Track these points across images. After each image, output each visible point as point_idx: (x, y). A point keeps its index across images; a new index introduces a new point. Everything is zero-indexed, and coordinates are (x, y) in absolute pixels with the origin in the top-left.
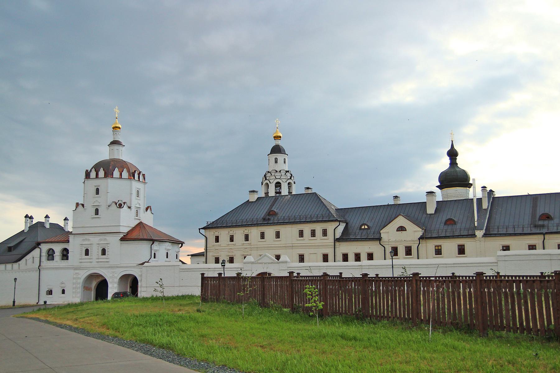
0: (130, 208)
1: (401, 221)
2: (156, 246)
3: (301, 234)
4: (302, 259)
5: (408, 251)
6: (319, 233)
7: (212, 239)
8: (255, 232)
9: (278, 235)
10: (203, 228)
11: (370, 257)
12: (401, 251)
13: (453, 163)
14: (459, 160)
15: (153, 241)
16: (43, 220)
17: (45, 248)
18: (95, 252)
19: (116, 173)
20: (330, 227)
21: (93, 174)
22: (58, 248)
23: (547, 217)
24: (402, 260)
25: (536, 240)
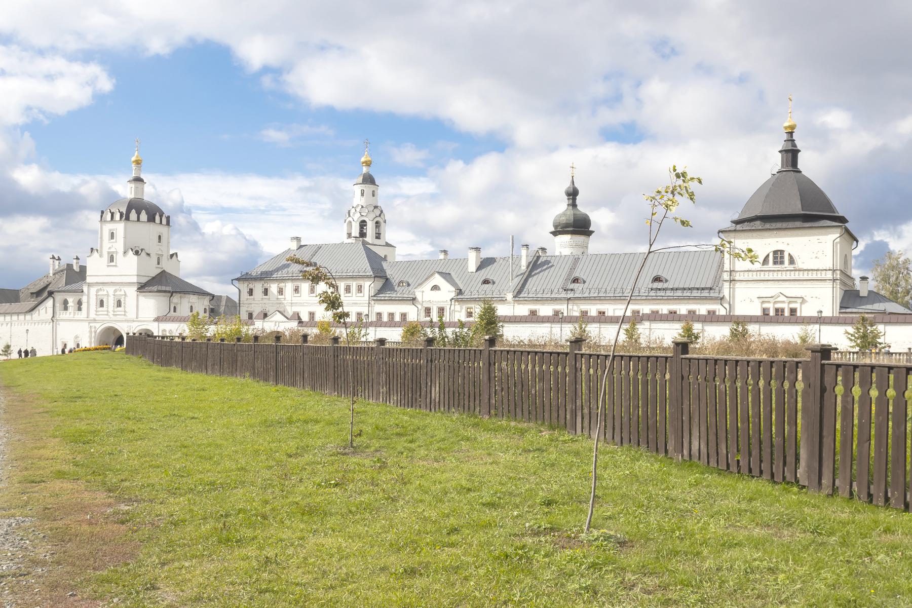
0: (148, 255)
2: (176, 299)
10: (237, 279)
13: (574, 205)
14: (579, 199)
17: (59, 297)
18: (110, 303)
19: (133, 215)
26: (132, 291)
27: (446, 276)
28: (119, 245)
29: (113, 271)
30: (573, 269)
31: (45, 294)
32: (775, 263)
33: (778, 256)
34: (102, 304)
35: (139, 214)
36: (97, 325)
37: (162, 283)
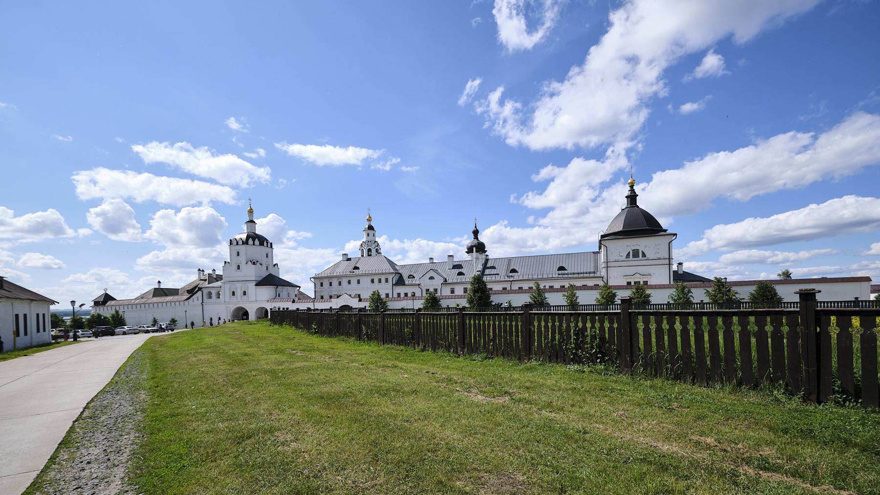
3: (373, 281)
6: (383, 280)
7: (319, 284)
9: (359, 282)
13: (476, 237)
16: (211, 272)
18: (239, 293)
28: (242, 259)
29: (239, 273)
32: (634, 256)
33: (636, 254)
36: (231, 306)
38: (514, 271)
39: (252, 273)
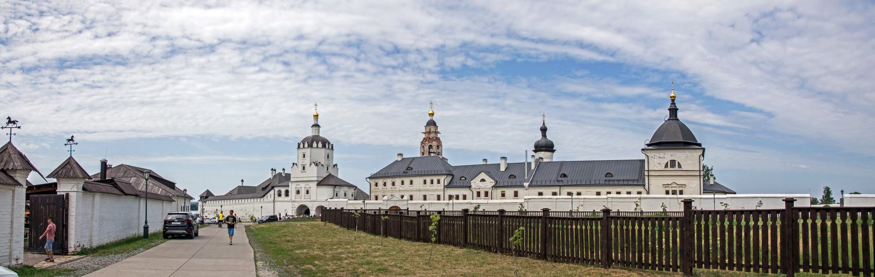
1: (483, 175)
2: (337, 189)
3: (425, 182)
4: (425, 198)
5: (486, 194)
6: (435, 181)
8: (398, 181)
9: (411, 183)
11: (465, 197)
12: (482, 194)
15: (335, 186)
17: (277, 189)
18: (303, 192)
19: (315, 145)
20: (442, 178)
21: (302, 146)
22: (283, 190)
23: (565, 176)
24: (482, 200)
25: (557, 190)
26: (313, 185)
27: (488, 174)
28: (307, 162)
29: (304, 175)
30: (560, 169)
31: (270, 187)
33: (673, 163)
34: (298, 192)
35: (317, 143)
37: (329, 181)
38: (565, 176)
39: (313, 173)
